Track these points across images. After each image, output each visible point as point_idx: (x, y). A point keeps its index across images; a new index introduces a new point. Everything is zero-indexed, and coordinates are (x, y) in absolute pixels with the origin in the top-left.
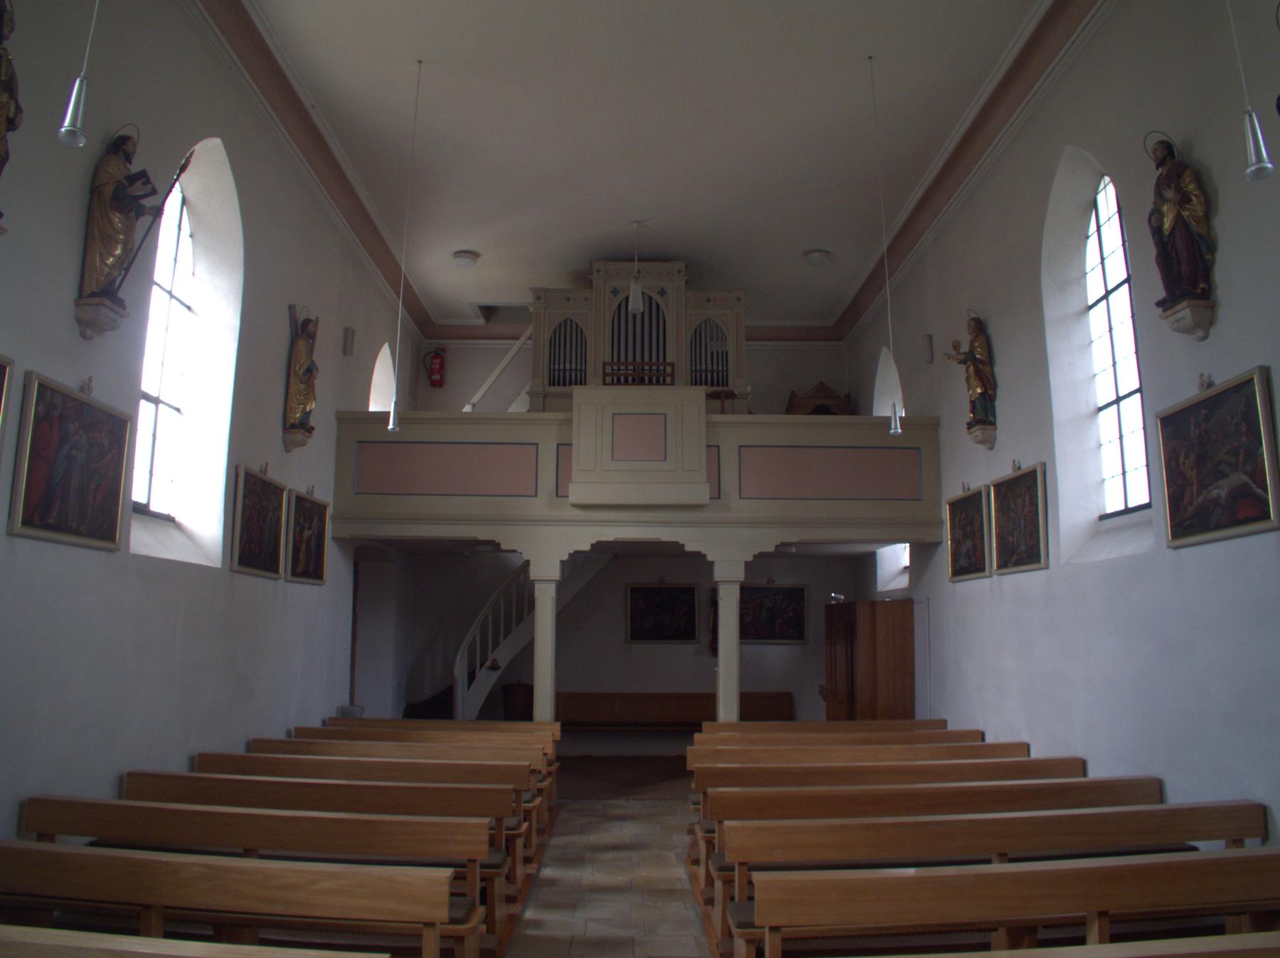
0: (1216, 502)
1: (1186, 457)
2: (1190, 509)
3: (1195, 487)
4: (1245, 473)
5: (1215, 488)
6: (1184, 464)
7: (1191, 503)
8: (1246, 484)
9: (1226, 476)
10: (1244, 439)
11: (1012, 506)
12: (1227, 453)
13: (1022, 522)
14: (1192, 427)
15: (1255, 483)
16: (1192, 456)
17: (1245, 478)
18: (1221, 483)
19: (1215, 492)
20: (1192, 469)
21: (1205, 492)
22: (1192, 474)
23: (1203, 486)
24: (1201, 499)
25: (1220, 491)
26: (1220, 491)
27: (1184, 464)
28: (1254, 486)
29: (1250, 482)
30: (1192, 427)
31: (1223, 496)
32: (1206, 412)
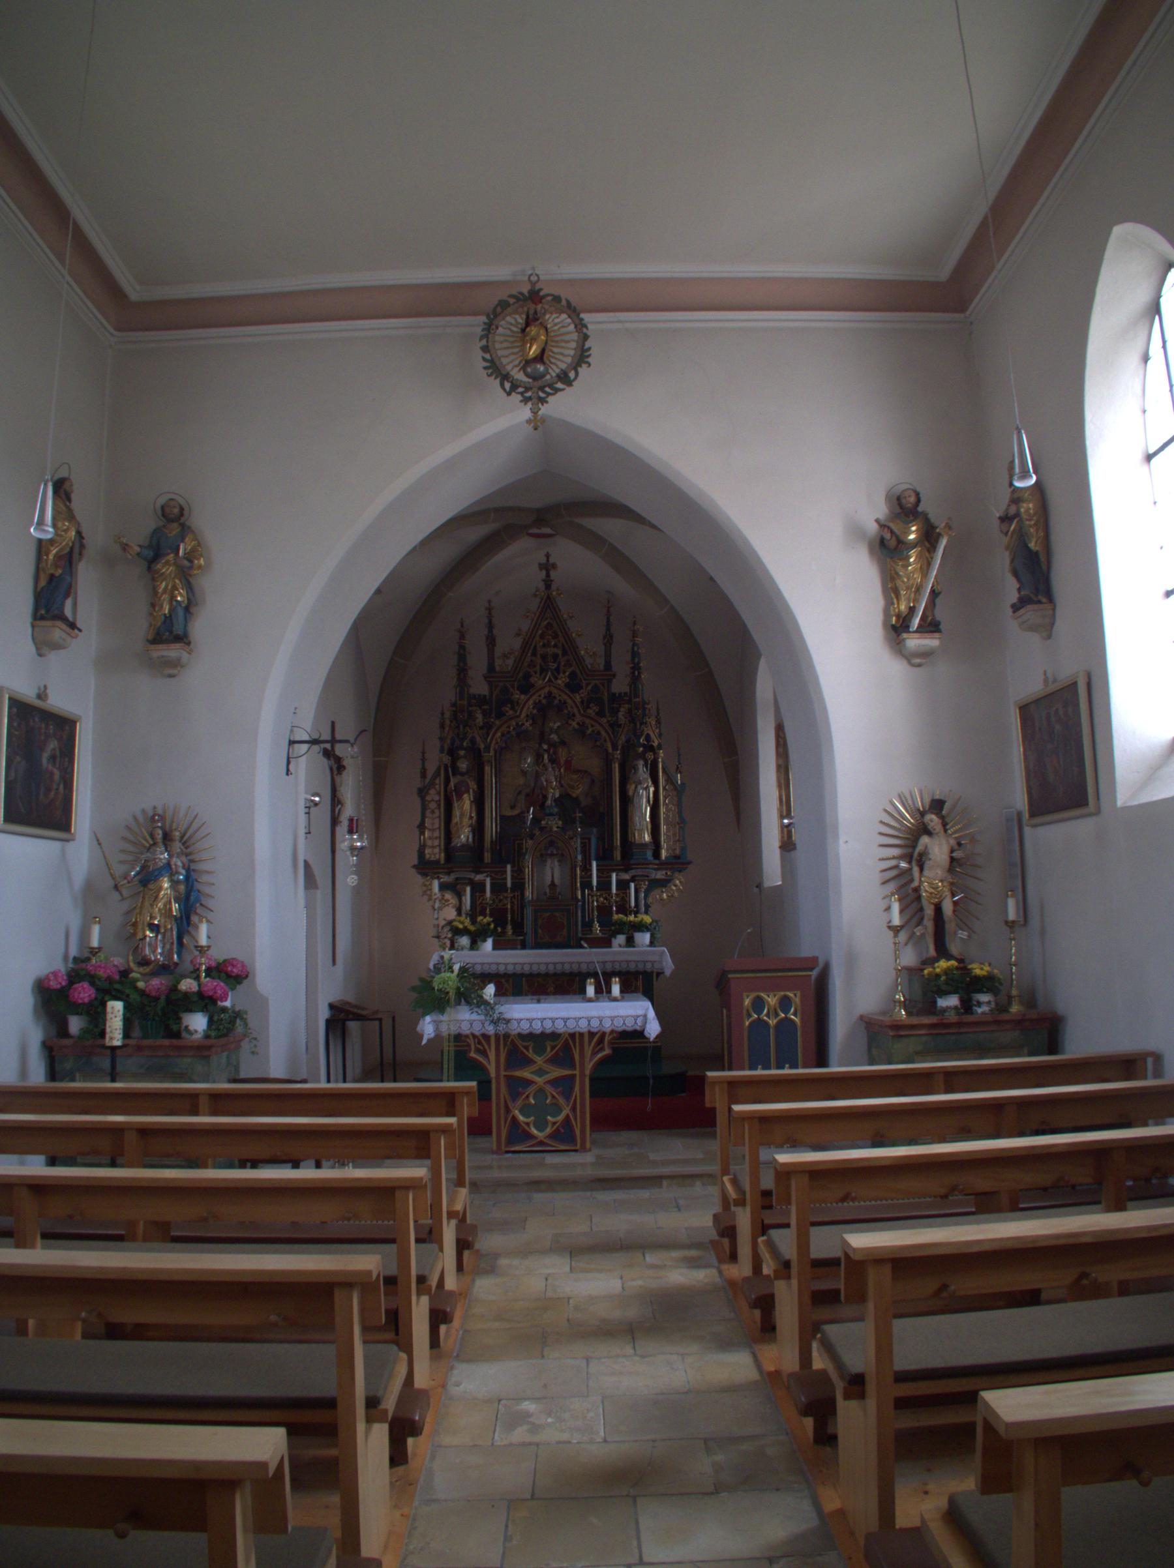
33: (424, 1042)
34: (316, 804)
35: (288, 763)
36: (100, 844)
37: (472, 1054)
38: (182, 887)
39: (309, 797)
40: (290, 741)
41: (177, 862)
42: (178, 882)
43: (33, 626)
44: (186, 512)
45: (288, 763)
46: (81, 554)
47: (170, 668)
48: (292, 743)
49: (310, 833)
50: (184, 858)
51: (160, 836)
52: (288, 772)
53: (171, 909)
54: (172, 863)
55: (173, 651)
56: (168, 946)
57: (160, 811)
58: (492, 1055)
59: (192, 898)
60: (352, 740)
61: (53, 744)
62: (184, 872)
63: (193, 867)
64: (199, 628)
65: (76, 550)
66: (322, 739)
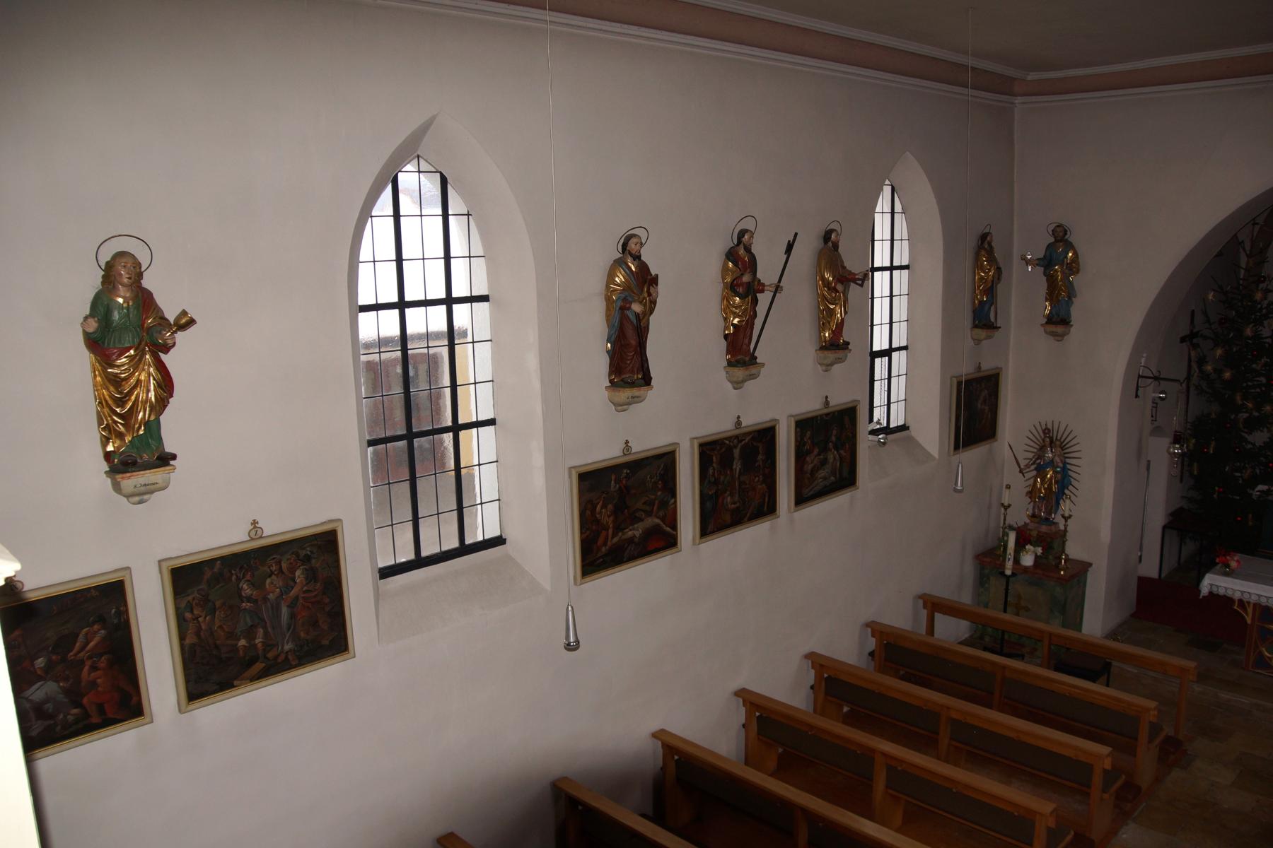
0: (631, 540)
1: (604, 506)
2: (604, 549)
3: (610, 531)
4: (658, 518)
5: (631, 530)
6: (601, 513)
7: (605, 544)
8: (658, 525)
9: (641, 520)
10: (659, 493)
11: (246, 589)
12: (644, 503)
13: (285, 611)
14: (613, 482)
15: (664, 524)
16: (610, 506)
17: (658, 521)
18: (636, 526)
19: (630, 533)
20: (609, 516)
21: (620, 534)
22: (608, 520)
23: (618, 528)
24: (615, 540)
25: (636, 531)
26: (636, 531)
27: (601, 513)
28: (664, 526)
29: (661, 523)
30: (613, 482)
31: (638, 535)
32: (628, 471)
33: (1201, 597)
34: (1162, 399)
35: (1137, 390)
36: (1011, 449)
37: (1235, 608)
38: (1059, 476)
39: (1157, 395)
40: (1139, 375)
41: (1057, 459)
42: (1057, 472)
43: (971, 331)
44: (1068, 233)
45: (1137, 390)
46: (999, 279)
47: (1059, 337)
48: (1140, 376)
49: (1156, 421)
50: (1062, 458)
51: (1049, 442)
52: (1137, 396)
53: (1052, 488)
54: (1054, 461)
55: (1060, 329)
56: (1049, 507)
57: (1050, 427)
58: (1250, 610)
59: (1066, 481)
60: (1182, 381)
61: (985, 393)
62: (1061, 465)
63: (1068, 461)
64: (1076, 312)
65: (996, 280)
66: (1162, 376)
